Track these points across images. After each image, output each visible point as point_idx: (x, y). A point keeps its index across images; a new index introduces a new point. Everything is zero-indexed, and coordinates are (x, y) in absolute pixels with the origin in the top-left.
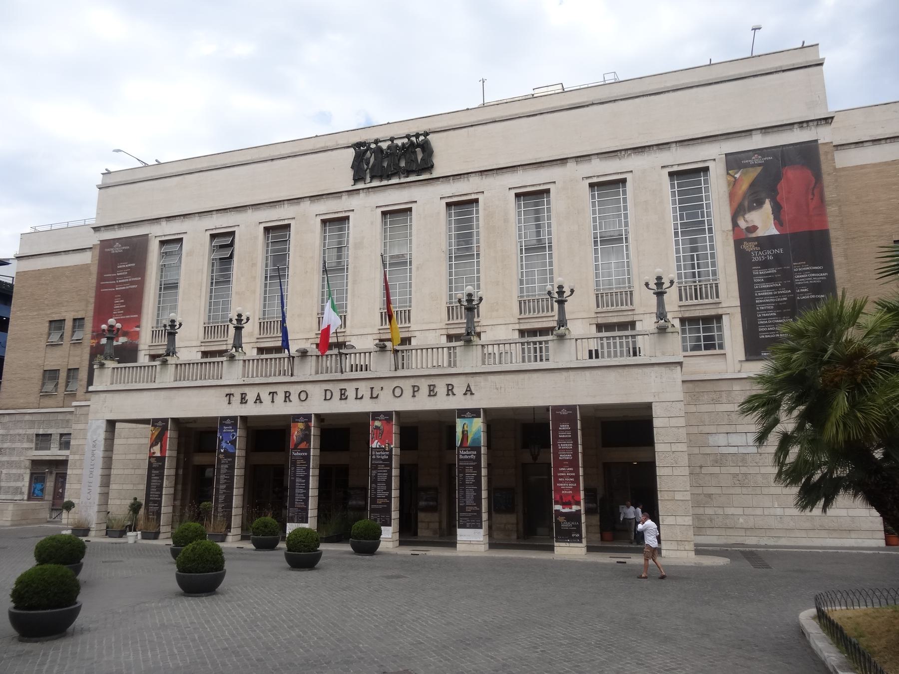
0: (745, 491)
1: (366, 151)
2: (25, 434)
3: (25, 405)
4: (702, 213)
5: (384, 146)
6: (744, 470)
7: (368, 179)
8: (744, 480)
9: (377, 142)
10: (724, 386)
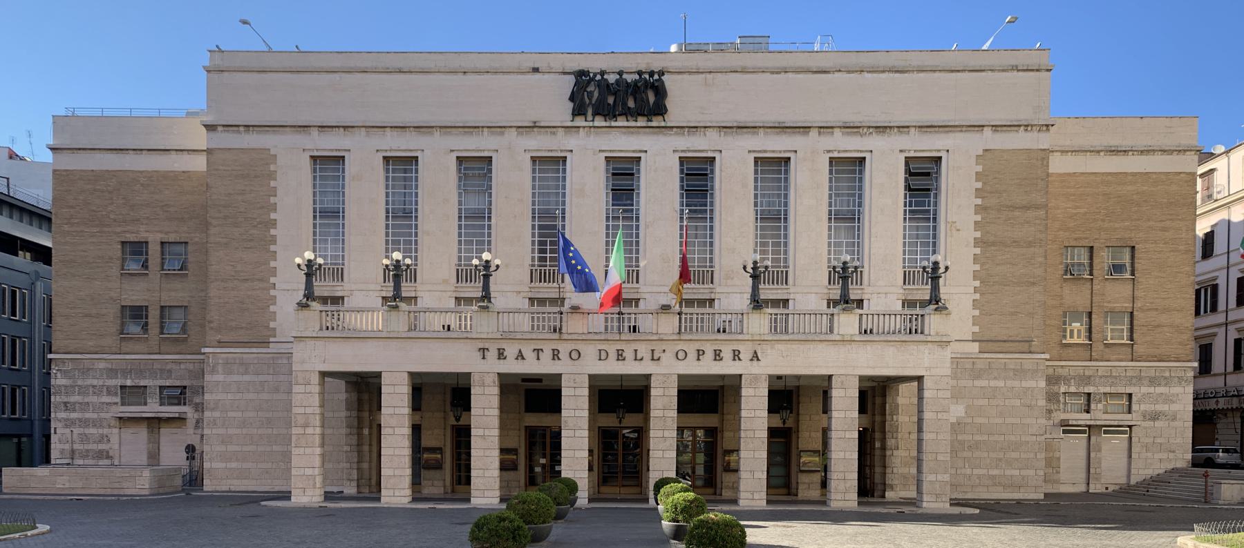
1: (589, 82)
2: (102, 386)
3: (97, 350)
4: (929, 202)
5: (612, 78)
7: (590, 117)
9: (603, 73)
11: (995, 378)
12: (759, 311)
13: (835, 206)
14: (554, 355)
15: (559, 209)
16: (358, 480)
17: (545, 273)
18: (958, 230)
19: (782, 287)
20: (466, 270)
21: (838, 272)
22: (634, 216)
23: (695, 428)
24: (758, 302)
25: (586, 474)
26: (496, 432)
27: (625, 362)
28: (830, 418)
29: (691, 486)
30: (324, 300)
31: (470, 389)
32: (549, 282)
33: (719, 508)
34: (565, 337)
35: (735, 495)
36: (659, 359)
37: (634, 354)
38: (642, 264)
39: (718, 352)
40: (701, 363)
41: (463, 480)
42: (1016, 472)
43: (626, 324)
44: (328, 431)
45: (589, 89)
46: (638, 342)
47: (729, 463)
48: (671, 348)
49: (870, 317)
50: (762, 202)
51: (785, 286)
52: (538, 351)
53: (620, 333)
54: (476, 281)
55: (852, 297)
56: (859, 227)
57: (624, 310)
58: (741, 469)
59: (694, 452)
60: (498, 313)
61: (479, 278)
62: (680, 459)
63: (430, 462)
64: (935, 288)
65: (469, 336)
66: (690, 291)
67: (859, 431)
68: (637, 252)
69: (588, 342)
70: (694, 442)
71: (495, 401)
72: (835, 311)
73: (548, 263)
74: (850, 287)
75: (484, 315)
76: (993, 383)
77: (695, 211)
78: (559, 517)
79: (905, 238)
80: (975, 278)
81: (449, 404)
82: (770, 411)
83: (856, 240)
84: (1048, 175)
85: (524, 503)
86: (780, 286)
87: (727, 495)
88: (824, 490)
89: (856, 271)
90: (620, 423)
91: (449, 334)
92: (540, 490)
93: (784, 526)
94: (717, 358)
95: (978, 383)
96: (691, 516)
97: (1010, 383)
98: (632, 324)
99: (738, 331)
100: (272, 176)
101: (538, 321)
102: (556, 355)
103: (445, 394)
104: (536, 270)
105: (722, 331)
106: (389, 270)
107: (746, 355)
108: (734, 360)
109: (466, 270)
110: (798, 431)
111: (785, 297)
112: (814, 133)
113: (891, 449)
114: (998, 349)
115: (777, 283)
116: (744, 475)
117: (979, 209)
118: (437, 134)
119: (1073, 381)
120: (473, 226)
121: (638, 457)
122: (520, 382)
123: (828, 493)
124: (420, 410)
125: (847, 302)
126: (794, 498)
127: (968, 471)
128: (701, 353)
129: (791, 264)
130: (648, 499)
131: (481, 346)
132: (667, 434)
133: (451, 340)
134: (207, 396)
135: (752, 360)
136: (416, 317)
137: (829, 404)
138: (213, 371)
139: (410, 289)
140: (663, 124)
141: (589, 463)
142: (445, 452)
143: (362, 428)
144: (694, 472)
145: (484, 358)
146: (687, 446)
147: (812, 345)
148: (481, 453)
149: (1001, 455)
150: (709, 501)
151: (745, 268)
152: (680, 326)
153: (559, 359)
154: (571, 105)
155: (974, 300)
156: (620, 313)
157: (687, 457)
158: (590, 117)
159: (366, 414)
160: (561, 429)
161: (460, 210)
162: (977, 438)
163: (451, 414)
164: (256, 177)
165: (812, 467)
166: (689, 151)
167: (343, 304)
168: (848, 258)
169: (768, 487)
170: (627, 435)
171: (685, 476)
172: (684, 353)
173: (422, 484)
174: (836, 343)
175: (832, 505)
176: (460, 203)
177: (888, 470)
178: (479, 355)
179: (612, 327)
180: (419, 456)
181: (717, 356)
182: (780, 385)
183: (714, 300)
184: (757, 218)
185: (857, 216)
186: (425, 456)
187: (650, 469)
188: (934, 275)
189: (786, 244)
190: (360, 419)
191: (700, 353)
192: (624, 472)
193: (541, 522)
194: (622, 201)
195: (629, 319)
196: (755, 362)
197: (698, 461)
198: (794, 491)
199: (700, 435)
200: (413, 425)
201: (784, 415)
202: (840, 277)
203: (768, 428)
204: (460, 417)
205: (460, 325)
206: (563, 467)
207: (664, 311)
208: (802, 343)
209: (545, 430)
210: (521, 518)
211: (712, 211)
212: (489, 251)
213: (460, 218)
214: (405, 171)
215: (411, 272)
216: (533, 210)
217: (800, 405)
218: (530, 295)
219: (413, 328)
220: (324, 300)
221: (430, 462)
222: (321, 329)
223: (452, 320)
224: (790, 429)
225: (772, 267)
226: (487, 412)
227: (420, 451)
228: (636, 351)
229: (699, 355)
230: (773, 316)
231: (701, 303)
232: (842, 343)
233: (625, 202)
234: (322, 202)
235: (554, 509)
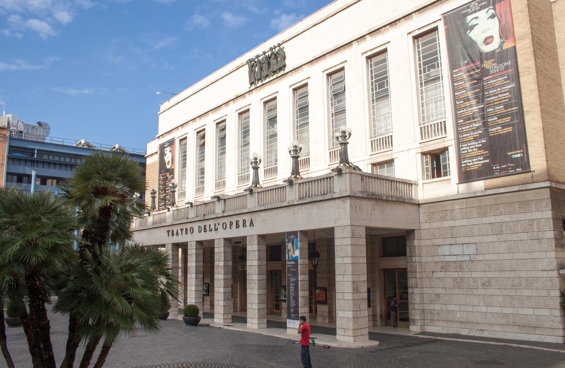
0: (461, 292)
6: (461, 274)
8: (461, 283)
10: (448, 205)
11: (501, 214)
42: (530, 312)
76: (499, 219)
97: (515, 217)
113: (412, 288)
149: (513, 293)
162: (490, 275)
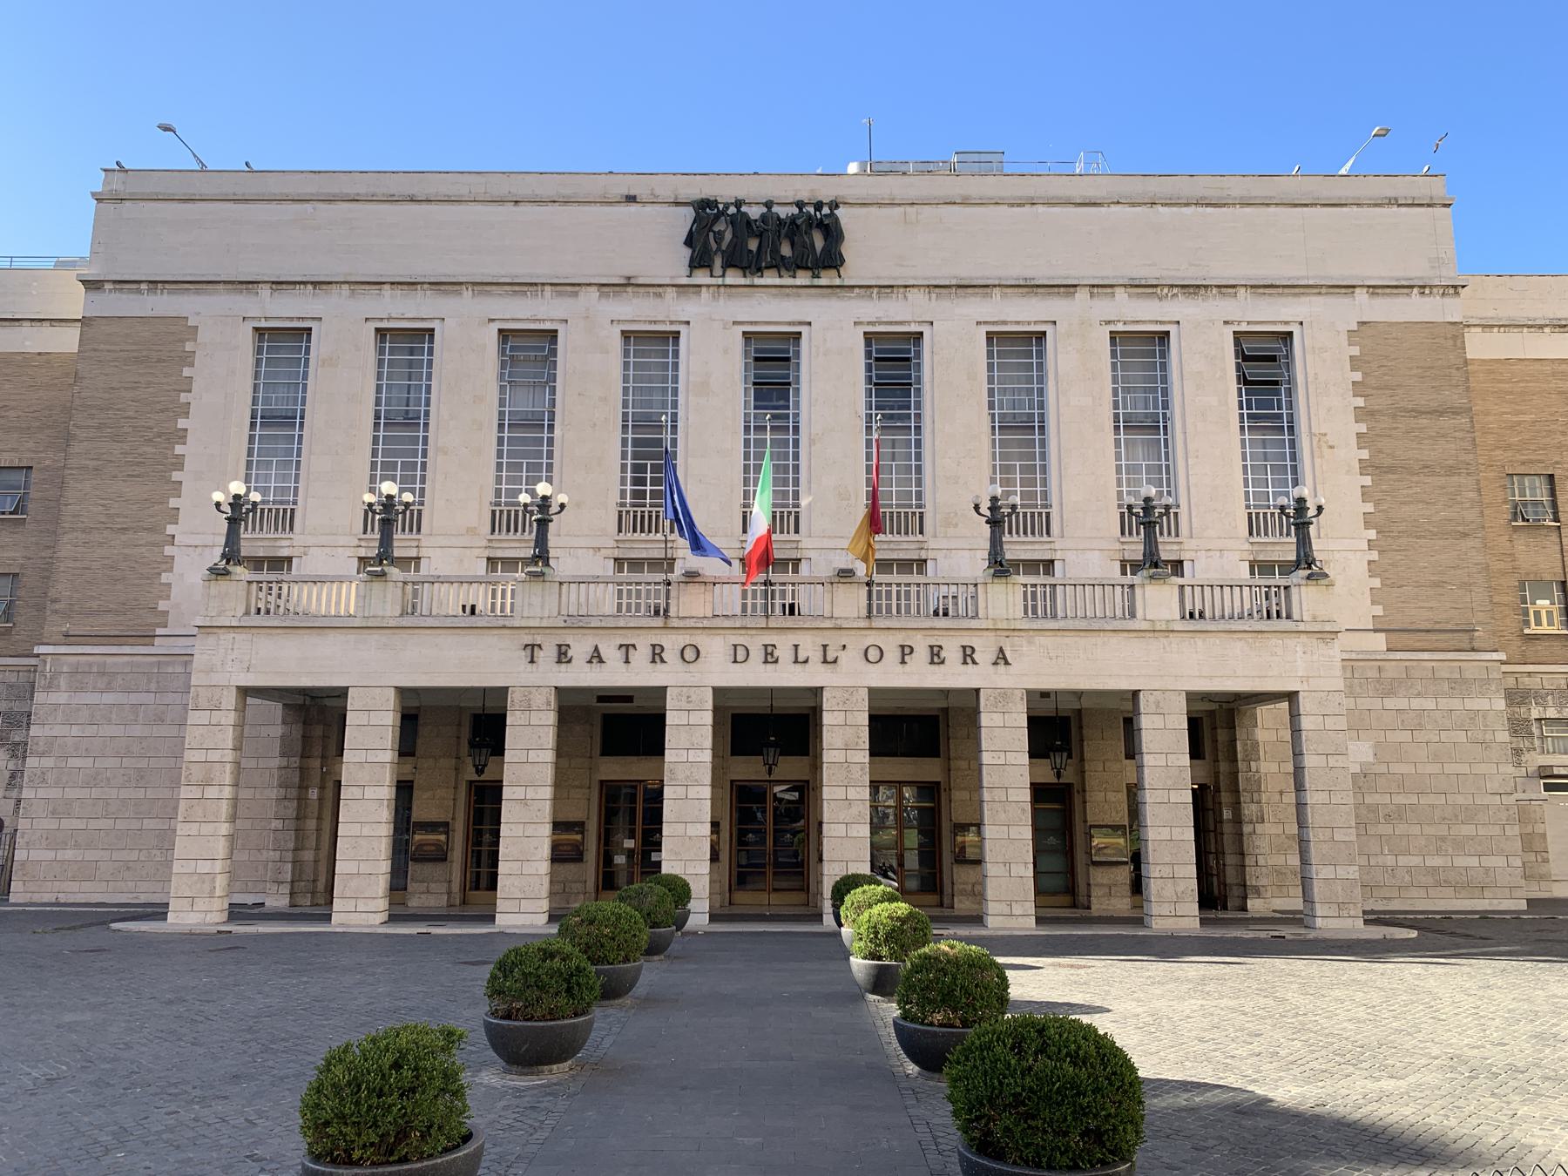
1: (717, 217)
4: (1279, 401)
5: (755, 212)
7: (718, 270)
9: (739, 204)
11: (1419, 695)
12: (1004, 580)
13: (1124, 408)
14: (654, 654)
15: (666, 414)
16: (292, 882)
17: (643, 517)
18: (1332, 447)
19: (1042, 539)
20: (509, 511)
21: (1137, 515)
22: (791, 424)
23: (899, 782)
24: (1001, 565)
25: (705, 867)
26: (547, 792)
27: (778, 666)
28: (1140, 767)
29: (897, 890)
30: (257, 563)
31: (504, 717)
32: (650, 531)
33: (951, 932)
34: (675, 623)
35: (976, 907)
36: (835, 661)
37: (793, 652)
38: (804, 502)
39: (936, 649)
40: (907, 667)
41: (484, 882)
42: (1474, 862)
43: (778, 602)
44: (245, 794)
45: (716, 228)
46: (798, 632)
47: (963, 849)
48: (857, 643)
49: (1198, 590)
50: (1001, 402)
51: (1045, 538)
52: (627, 648)
53: (767, 617)
54: (524, 531)
55: (1164, 556)
56: (1166, 440)
57: (774, 577)
58: (987, 860)
59: (901, 825)
60: (561, 583)
61: (530, 525)
62: (876, 838)
63: (425, 848)
64: (1304, 542)
65: (508, 624)
66: (885, 546)
67: (1193, 789)
68: (796, 482)
69: (713, 631)
70: (900, 808)
71: (549, 737)
72: (1137, 579)
73: (648, 501)
74: (1160, 539)
75: (537, 587)
76: (1416, 703)
77: (891, 417)
78: (655, 949)
79: (1244, 459)
80: (1368, 525)
81: (467, 744)
82: (1034, 753)
83: (1164, 463)
84: (1466, 362)
85: (591, 922)
86: (1037, 538)
87: (962, 906)
88: (1137, 898)
89: (1167, 513)
90: (770, 774)
91: (473, 621)
92: (621, 899)
93: (1072, 966)
94: (936, 659)
95: (1390, 703)
96: (905, 949)
97: (1444, 703)
98: (788, 601)
99: (970, 616)
100: (188, 359)
101: (629, 597)
102: (657, 655)
103: (459, 725)
104: (628, 512)
105: (941, 613)
106: (374, 512)
107: (984, 655)
108: (965, 663)
109: (509, 511)
110: (1084, 791)
111: (1048, 557)
112: (1082, 295)
113: (1251, 822)
114: (1418, 645)
115: (1033, 533)
116: (992, 869)
117: (1361, 414)
118: (467, 294)
119: (1549, 697)
120: (524, 441)
121: (800, 836)
122: (594, 702)
123: (1145, 904)
124: (413, 755)
125: (1156, 566)
126: (1084, 913)
127: (1390, 860)
128: (907, 650)
129: (1054, 500)
130: (821, 915)
131: (528, 640)
132: (852, 793)
133: (476, 631)
134: (34, 731)
135: (995, 663)
136: (415, 593)
137: (1136, 741)
138: (50, 687)
139: (408, 544)
140: (837, 282)
141: (712, 847)
142: (454, 831)
143: (307, 788)
144: (901, 864)
145: (532, 661)
146: (886, 816)
147: (1099, 639)
148: (518, 831)
150: (934, 919)
151: (977, 508)
152: (870, 606)
153: (662, 661)
154: (687, 252)
155: (1370, 562)
156: (767, 583)
157: (889, 835)
158: (718, 270)
159: (316, 763)
160: (663, 785)
161: (501, 414)
162: (1400, 799)
163: (469, 760)
164: (159, 361)
165: (1110, 855)
166: (881, 323)
167: (289, 569)
168: (1153, 491)
169: (1038, 892)
170: (779, 795)
171: (886, 871)
172: (878, 652)
173: (410, 889)
174: (1142, 634)
175: (1154, 926)
176: (502, 403)
177: (1249, 861)
178: (524, 655)
179: (754, 605)
180: (407, 837)
181: (936, 656)
182: (1046, 709)
183: (925, 561)
184: (994, 427)
185: (1161, 424)
186: (417, 837)
187: (825, 858)
188: (1300, 519)
189: (1044, 469)
190: (303, 771)
191: (906, 651)
192: (777, 864)
193: (620, 958)
194: (772, 401)
195: (783, 593)
196: (1002, 667)
197: (907, 844)
198: (1082, 899)
199: (907, 795)
200: (398, 781)
201: (1058, 761)
202: (1141, 524)
203: (1031, 784)
204: (485, 765)
205: (493, 604)
206: (664, 854)
207: (842, 580)
208: (1082, 634)
209: (635, 787)
210: (586, 952)
211: (918, 416)
212: (549, 480)
213: (501, 426)
214: (412, 352)
215: (412, 515)
216: (625, 415)
217: (1085, 743)
218: (617, 554)
219: (409, 611)
220: (257, 563)
221: (425, 848)
222: (247, 613)
223: (479, 596)
224: (1069, 786)
225: (1023, 506)
226: (533, 756)
227: (408, 830)
228: (796, 646)
229: (903, 655)
230: (1029, 589)
231: (905, 566)
232: (1152, 635)
233: (775, 403)
234: (266, 400)
235: (645, 937)
